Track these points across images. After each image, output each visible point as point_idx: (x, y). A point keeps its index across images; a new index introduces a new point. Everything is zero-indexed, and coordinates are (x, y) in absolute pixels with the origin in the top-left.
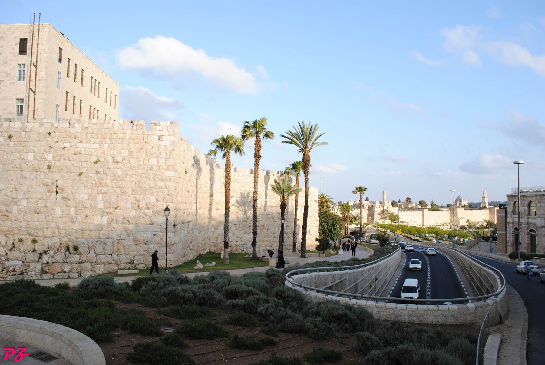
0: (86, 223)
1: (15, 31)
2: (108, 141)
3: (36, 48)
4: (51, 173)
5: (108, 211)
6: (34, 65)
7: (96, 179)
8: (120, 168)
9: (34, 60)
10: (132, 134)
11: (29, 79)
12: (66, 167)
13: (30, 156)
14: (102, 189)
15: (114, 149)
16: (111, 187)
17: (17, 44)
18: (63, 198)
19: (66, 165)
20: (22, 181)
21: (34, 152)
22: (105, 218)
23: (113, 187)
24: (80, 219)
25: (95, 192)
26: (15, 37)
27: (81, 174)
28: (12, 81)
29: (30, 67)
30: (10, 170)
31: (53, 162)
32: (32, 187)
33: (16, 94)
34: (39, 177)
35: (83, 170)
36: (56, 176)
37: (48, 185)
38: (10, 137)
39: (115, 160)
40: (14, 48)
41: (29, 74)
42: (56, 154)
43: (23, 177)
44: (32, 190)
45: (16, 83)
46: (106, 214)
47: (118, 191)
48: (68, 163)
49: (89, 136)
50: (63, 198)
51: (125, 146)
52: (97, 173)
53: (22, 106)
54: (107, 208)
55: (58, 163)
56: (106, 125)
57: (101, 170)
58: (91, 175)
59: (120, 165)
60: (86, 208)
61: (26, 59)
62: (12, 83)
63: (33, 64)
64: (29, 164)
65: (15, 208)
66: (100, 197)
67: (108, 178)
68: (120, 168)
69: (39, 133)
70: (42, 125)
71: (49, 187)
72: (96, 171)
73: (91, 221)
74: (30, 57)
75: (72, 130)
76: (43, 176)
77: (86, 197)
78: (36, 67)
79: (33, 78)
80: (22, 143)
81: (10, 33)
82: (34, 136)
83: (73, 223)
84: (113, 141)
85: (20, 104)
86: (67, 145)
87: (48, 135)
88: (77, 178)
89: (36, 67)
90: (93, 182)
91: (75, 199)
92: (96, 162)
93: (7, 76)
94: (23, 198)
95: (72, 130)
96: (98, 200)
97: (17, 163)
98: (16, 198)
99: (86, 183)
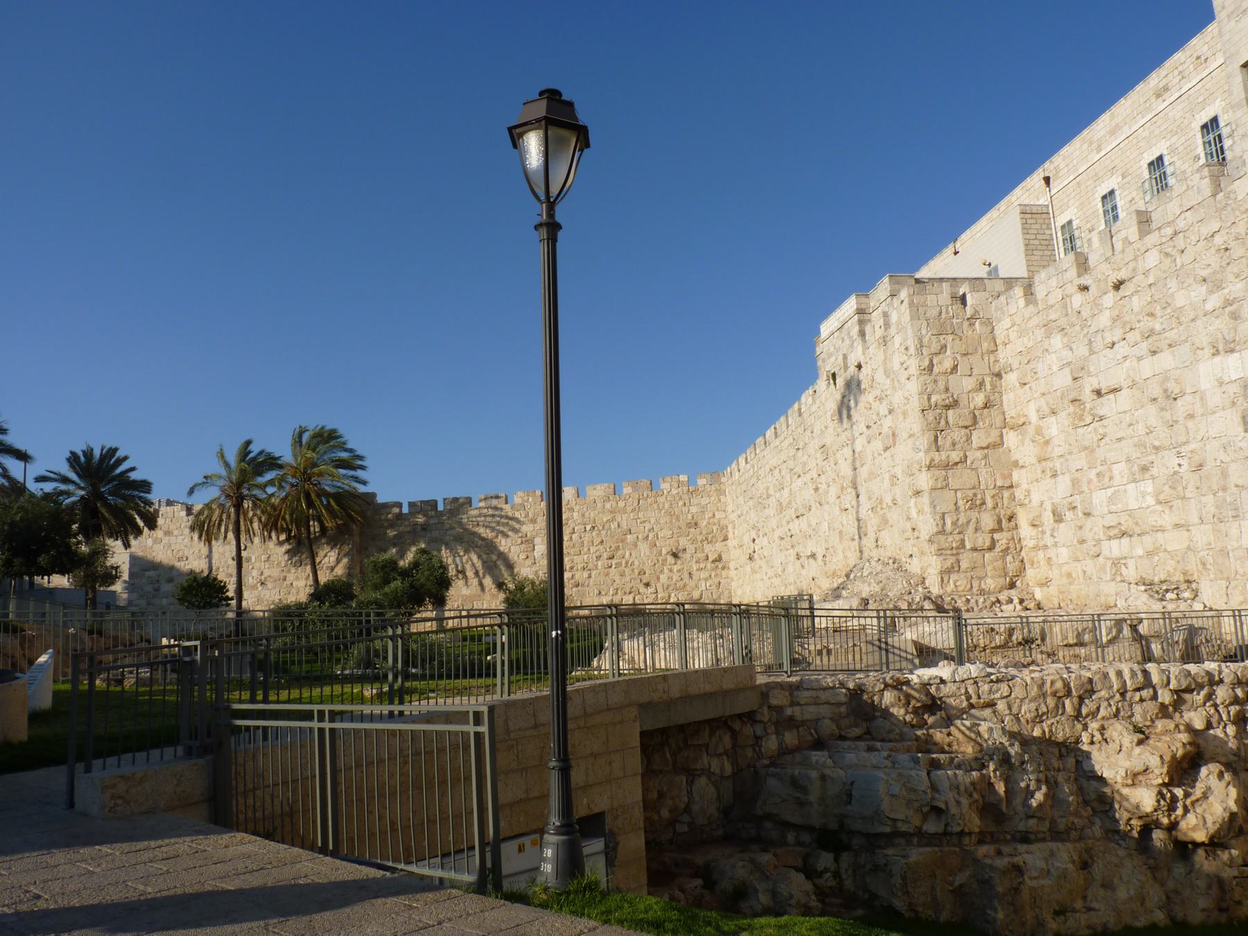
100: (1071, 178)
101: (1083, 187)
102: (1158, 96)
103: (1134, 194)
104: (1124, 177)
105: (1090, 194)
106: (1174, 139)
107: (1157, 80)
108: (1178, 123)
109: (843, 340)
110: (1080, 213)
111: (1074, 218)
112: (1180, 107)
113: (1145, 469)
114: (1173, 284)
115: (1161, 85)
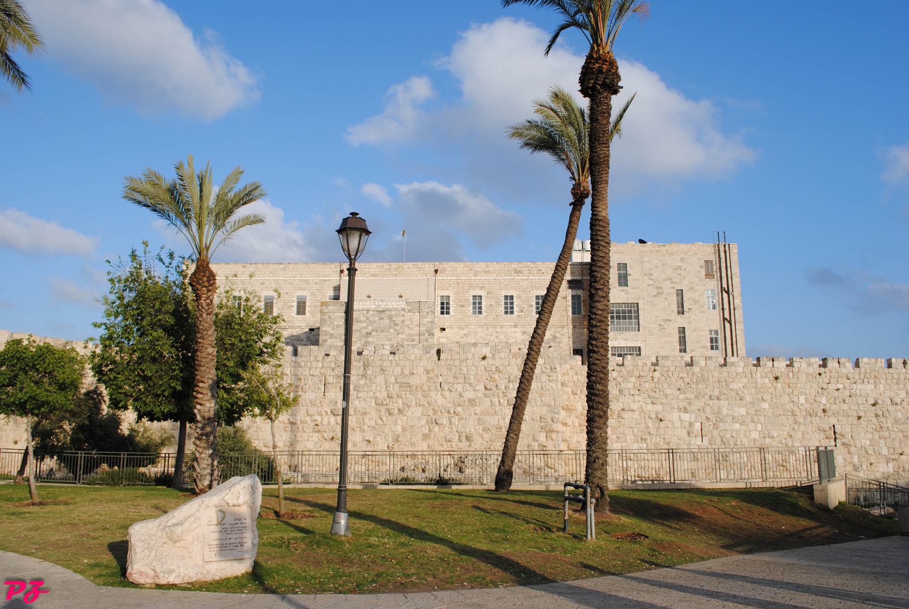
0: (872, 471)
1: (697, 251)
2: (883, 381)
3: (725, 272)
4: (827, 418)
5: (893, 457)
6: (725, 292)
7: (876, 423)
8: (899, 410)
9: (725, 285)
10: (907, 373)
11: (721, 307)
12: (843, 410)
13: (802, 400)
14: (883, 434)
15: (890, 390)
16: (893, 431)
17: (701, 267)
18: (843, 444)
19: (842, 408)
20: (796, 427)
21: (806, 394)
22: (891, 465)
23: (895, 432)
24: (864, 467)
25: (877, 437)
26: (698, 259)
27: (859, 418)
28: (702, 310)
29: (720, 293)
30: (781, 415)
31: (828, 406)
32: (808, 433)
33: (709, 325)
34: (814, 422)
35: (862, 414)
36: (833, 421)
37: (824, 431)
38: (776, 378)
39: (894, 402)
40: (699, 272)
41: (721, 301)
42: (829, 397)
43: (796, 422)
44: (809, 436)
45: (706, 312)
46: (891, 460)
47: (900, 435)
48: (844, 407)
49: (862, 377)
50: (843, 444)
51: (902, 386)
52: (877, 415)
53: (716, 339)
54: (892, 454)
55: (833, 407)
56: (878, 364)
57: (880, 413)
58: (872, 419)
59: (899, 407)
60: (870, 454)
61: (715, 285)
62: (702, 312)
63: (725, 290)
64: (801, 407)
65: (792, 459)
66: (882, 441)
67: (889, 421)
68: (899, 410)
69: (807, 374)
70: (809, 365)
71: (827, 433)
72: (876, 414)
73: (877, 469)
74: (719, 282)
75: (844, 371)
76: (818, 421)
77: (868, 443)
78: (728, 292)
79: (726, 306)
80: (791, 385)
81: (692, 254)
82: (803, 377)
83: (858, 471)
84: (889, 382)
85: (714, 336)
86: (840, 386)
87: (818, 376)
88: (856, 422)
89: (728, 292)
90: (874, 426)
91: (857, 446)
92: (874, 405)
93: (696, 304)
94: (799, 445)
95: (844, 371)
96: (881, 446)
97: (788, 407)
98: (793, 446)
99: (866, 428)
100: (455, 278)
101: (461, 285)
102: (515, 272)
103: (493, 303)
104: (488, 294)
105: (465, 290)
106: (521, 293)
107: (516, 266)
108: (523, 288)
109: (381, 319)
110: (456, 296)
111: (451, 296)
112: (526, 283)
113: (645, 440)
114: (665, 386)
115: (518, 269)
